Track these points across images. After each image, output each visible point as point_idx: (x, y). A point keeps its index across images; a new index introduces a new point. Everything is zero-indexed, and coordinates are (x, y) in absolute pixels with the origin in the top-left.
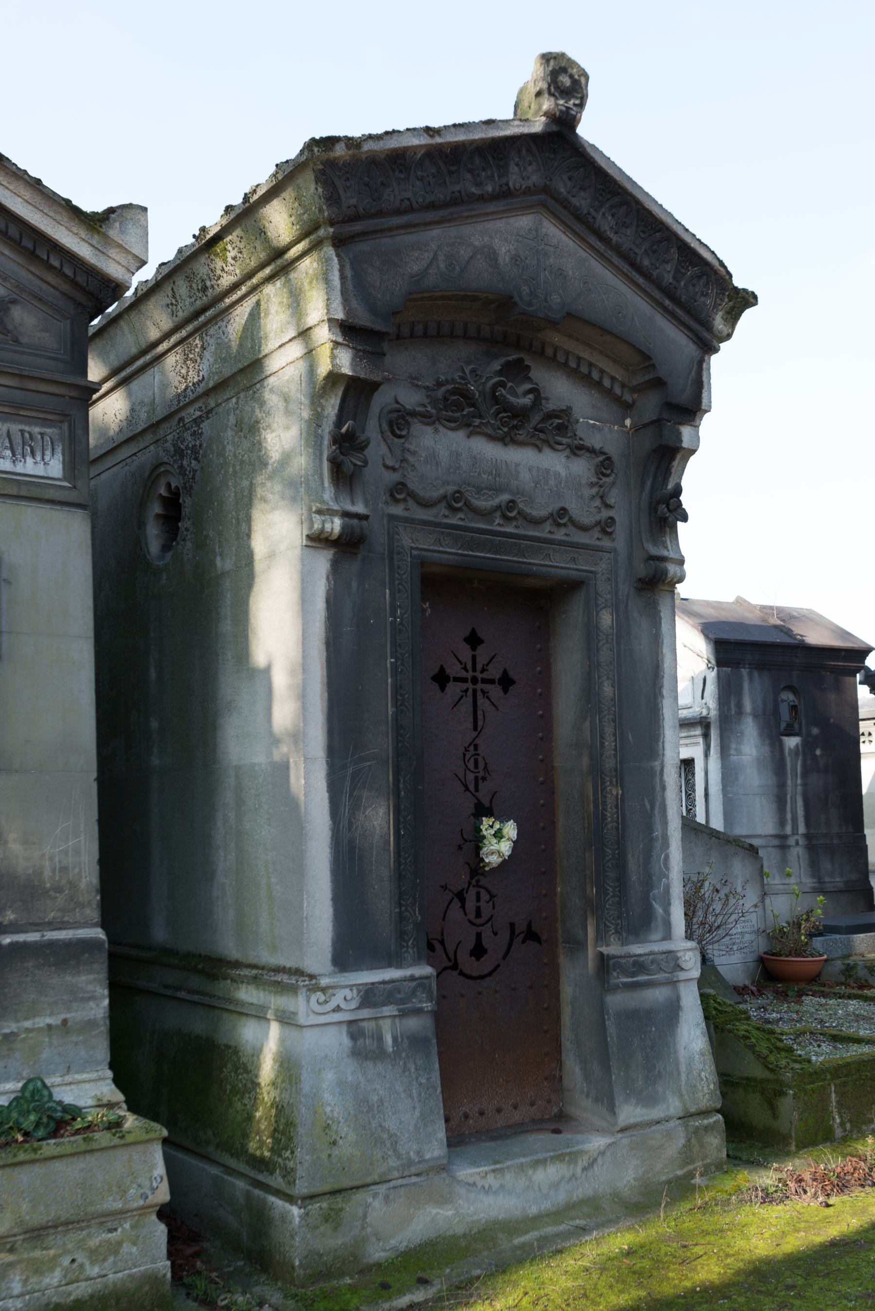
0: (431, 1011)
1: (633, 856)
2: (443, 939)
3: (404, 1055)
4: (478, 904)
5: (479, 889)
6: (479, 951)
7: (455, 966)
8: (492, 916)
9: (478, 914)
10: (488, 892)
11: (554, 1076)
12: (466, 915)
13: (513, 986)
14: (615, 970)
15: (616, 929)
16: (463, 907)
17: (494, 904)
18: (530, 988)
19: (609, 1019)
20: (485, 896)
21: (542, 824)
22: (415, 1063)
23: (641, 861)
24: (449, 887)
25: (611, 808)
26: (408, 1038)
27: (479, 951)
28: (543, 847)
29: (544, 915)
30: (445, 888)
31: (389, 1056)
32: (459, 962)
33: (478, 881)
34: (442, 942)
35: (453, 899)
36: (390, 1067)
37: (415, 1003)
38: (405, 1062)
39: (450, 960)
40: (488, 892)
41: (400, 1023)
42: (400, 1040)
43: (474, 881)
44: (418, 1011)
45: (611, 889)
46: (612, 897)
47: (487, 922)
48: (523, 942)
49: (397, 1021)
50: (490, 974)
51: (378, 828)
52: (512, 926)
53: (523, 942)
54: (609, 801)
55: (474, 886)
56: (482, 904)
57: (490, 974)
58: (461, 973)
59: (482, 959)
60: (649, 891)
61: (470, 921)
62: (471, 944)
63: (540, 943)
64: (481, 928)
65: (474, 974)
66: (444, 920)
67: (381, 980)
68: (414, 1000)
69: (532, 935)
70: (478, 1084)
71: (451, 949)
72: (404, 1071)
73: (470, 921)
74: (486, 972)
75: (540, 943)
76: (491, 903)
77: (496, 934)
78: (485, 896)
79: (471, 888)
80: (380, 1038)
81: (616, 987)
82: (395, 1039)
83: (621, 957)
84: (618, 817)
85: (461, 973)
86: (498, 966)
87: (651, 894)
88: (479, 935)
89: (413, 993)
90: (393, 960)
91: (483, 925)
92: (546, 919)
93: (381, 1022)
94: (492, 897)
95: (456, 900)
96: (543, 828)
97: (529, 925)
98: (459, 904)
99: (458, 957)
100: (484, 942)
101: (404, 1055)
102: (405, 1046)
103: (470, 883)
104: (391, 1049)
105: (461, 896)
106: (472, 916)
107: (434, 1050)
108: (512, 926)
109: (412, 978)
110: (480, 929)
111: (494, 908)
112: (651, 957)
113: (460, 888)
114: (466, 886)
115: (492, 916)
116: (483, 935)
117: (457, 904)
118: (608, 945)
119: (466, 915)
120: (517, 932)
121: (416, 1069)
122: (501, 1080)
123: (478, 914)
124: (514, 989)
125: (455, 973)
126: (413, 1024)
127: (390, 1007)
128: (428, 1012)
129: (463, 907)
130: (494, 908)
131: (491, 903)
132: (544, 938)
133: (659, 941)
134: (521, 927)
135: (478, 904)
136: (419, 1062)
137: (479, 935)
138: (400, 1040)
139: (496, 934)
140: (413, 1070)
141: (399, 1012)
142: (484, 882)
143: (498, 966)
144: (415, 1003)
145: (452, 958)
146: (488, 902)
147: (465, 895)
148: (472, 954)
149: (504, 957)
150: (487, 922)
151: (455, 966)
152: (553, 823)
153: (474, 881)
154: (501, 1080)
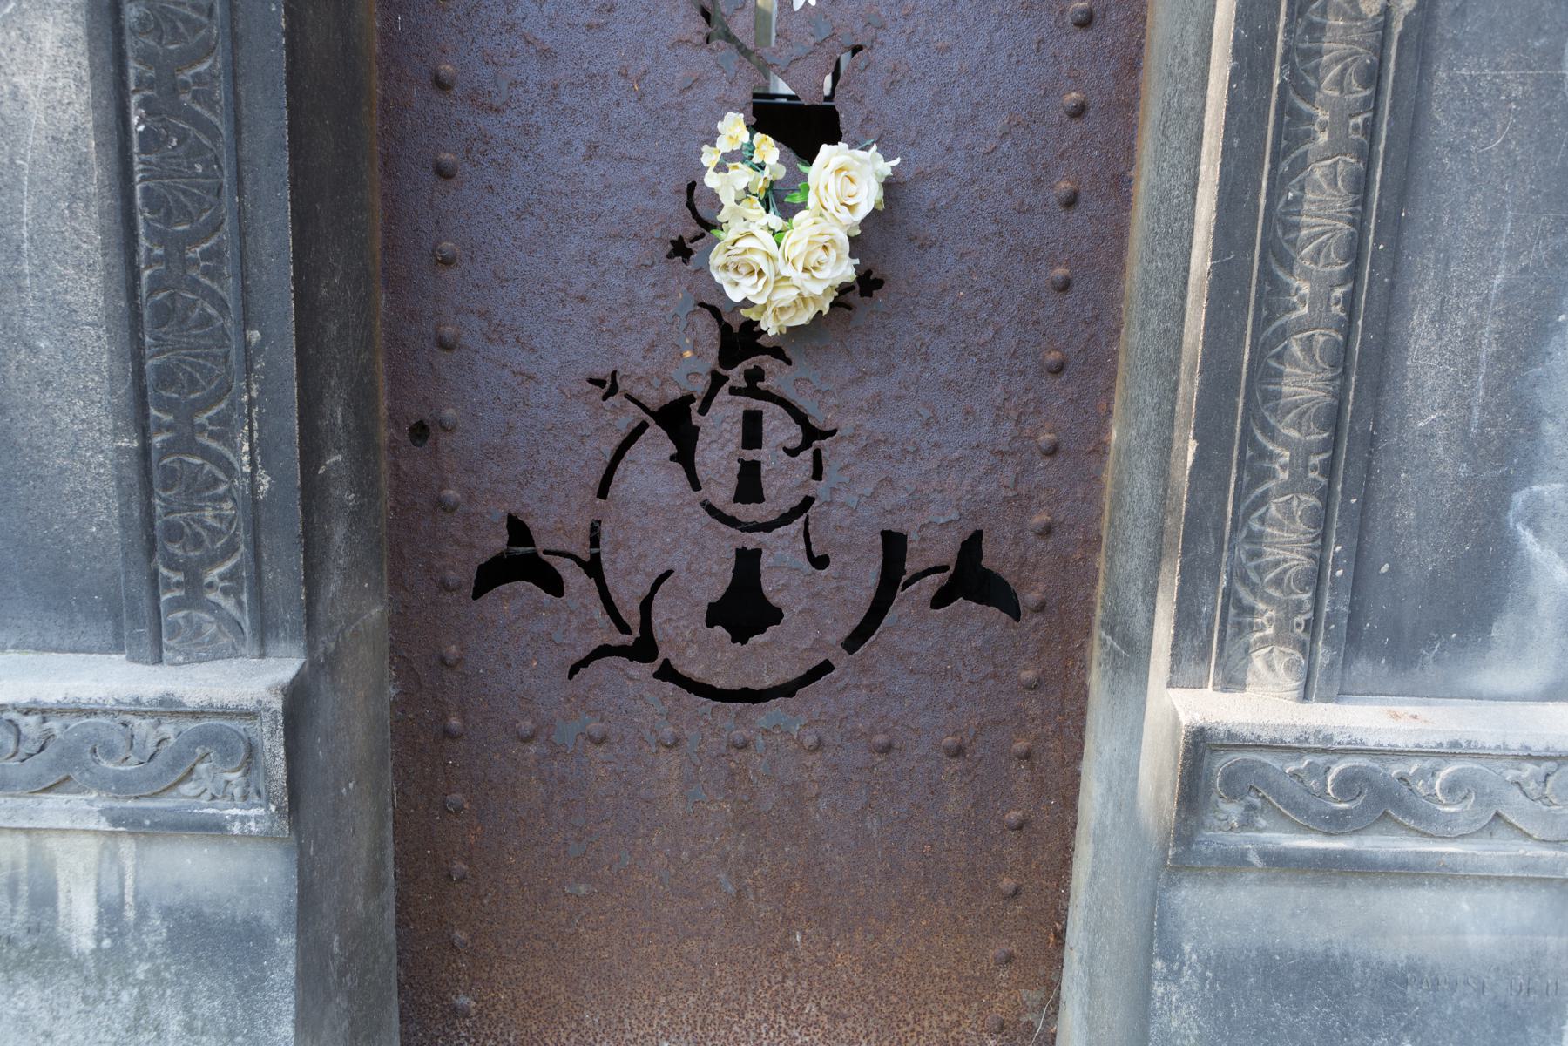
0: (267, 837)
1: (1440, 317)
2: (596, 558)
3: (141, 970)
4: (750, 455)
5: (755, 404)
6: (744, 609)
7: (644, 649)
8: (808, 502)
9: (750, 484)
10: (800, 418)
11: (1030, 1026)
12: (695, 485)
13: (880, 739)
14: (1232, 796)
15: (1283, 626)
16: (685, 456)
17: (817, 456)
18: (958, 752)
19: (1173, 976)
20: (779, 429)
21: (1064, 186)
22: (187, 1008)
23: (1487, 345)
24: (624, 385)
25: (1339, 83)
26: (168, 913)
27: (744, 609)
28: (1060, 272)
29: (1039, 519)
30: (608, 386)
31: (77, 965)
32: (658, 636)
33: (755, 375)
34: (593, 568)
35: (643, 426)
36: (77, 1004)
37: (190, 797)
38: (143, 997)
39: (624, 628)
40: (800, 418)
41: (139, 857)
42: (130, 914)
43: (736, 376)
44: (212, 829)
45: (1286, 456)
46: (1285, 488)
47: (786, 519)
48: (941, 599)
49: (127, 847)
50: (787, 690)
51: (36, 106)
52: (894, 544)
53: (941, 599)
54: (1332, 47)
55: (734, 391)
56: (768, 455)
57: (787, 690)
58: (667, 673)
59: (757, 639)
60: (1504, 488)
61: (711, 510)
62: (716, 582)
63: (1016, 615)
64: (759, 536)
65: (719, 683)
66: (603, 492)
67: (24, 699)
68: (188, 789)
69: (972, 579)
70: (718, 1007)
71: (628, 598)
72: (134, 1028)
73: (711, 510)
74: (768, 682)
75: (1016, 615)
76: (807, 455)
77: (820, 562)
78: (779, 429)
79: (723, 394)
80: (44, 899)
81: (1232, 864)
82: (109, 913)
83: (1273, 747)
84: (1371, 130)
85: (667, 673)
86: (825, 668)
87: (1519, 498)
88: (748, 562)
89: (181, 768)
90: (143, 627)
91: (768, 527)
92: (1047, 531)
93: (53, 844)
94: (812, 434)
95: (654, 430)
96: (1071, 202)
97: (972, 546)
98: (670, 448)
99: (656, 621)
100: (771, 585)
101: (141, 970)
102: (149, 940)
103: (717, 381)
104: (88, 944)
105: (677, 420)
106: (722, 493)
107: (284, 971)
108: (894, 544)
109: (169, 708)
110: (751, 540)
111: (817, 474)
112: (1447, 770)
113: (674, 393)
114: (700, 386)
115: (808, 502)
116: (766, 561)
117: (657, 445)
118: (1232, 681)
119: (695, 485)
120: (912, 566)
121: (189, 1028)
122: (811, 1008)
123: (750, 484)
124: (887, 749)
125: (647, 670)
126: (195, 869)
127: (78, 801)
128: (247, 836)
129: (685, 456)
130: (817, 474)
131: (807, 455)
132: (1029, 598)
133: (1525, 698)
134: (933, 547)
135: (750, 455)
136: (206, 1007)
137: (748, 562)
138: (130, 914)
139: (820, 562)
140: (174, 1027)
141: (114, 821)
142: (777, 378)
143: (825, 668)
144: (190, 797)
145: (634, 621)
146: (792, 453)
147: (696, 419)
148: (715, 615)
149: (855, 640)
150: (786, 519)
151: (644, 649)
152: (1120, 186)
153: (736, 376)
154: (811, 1008)
